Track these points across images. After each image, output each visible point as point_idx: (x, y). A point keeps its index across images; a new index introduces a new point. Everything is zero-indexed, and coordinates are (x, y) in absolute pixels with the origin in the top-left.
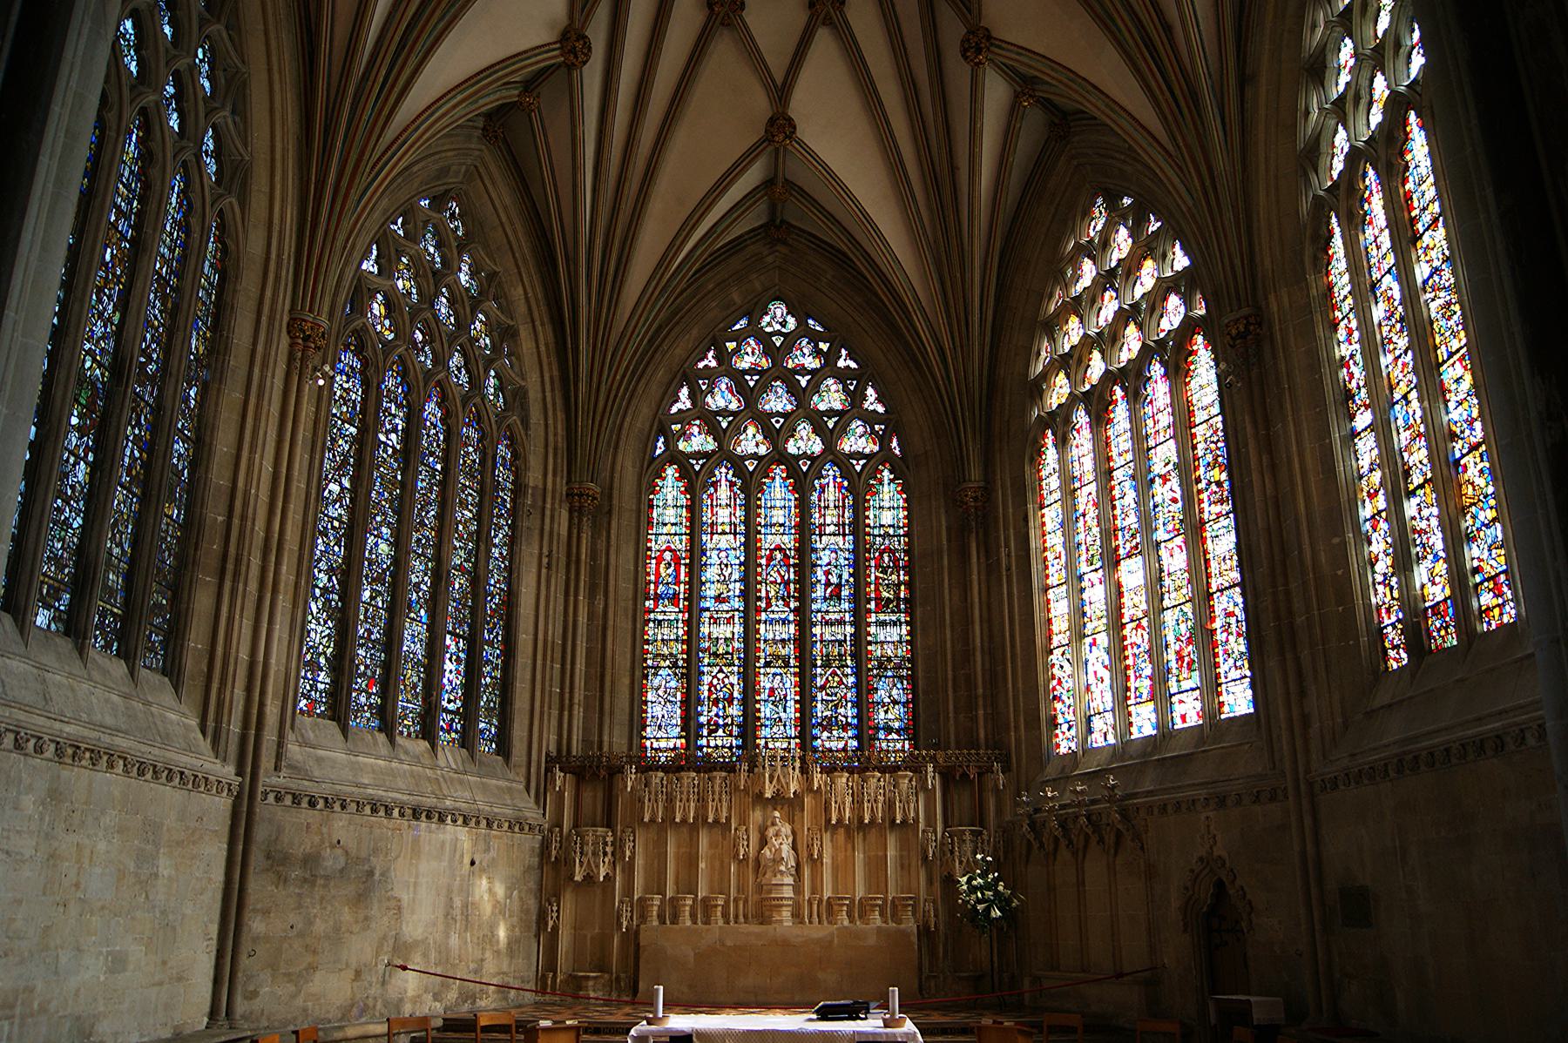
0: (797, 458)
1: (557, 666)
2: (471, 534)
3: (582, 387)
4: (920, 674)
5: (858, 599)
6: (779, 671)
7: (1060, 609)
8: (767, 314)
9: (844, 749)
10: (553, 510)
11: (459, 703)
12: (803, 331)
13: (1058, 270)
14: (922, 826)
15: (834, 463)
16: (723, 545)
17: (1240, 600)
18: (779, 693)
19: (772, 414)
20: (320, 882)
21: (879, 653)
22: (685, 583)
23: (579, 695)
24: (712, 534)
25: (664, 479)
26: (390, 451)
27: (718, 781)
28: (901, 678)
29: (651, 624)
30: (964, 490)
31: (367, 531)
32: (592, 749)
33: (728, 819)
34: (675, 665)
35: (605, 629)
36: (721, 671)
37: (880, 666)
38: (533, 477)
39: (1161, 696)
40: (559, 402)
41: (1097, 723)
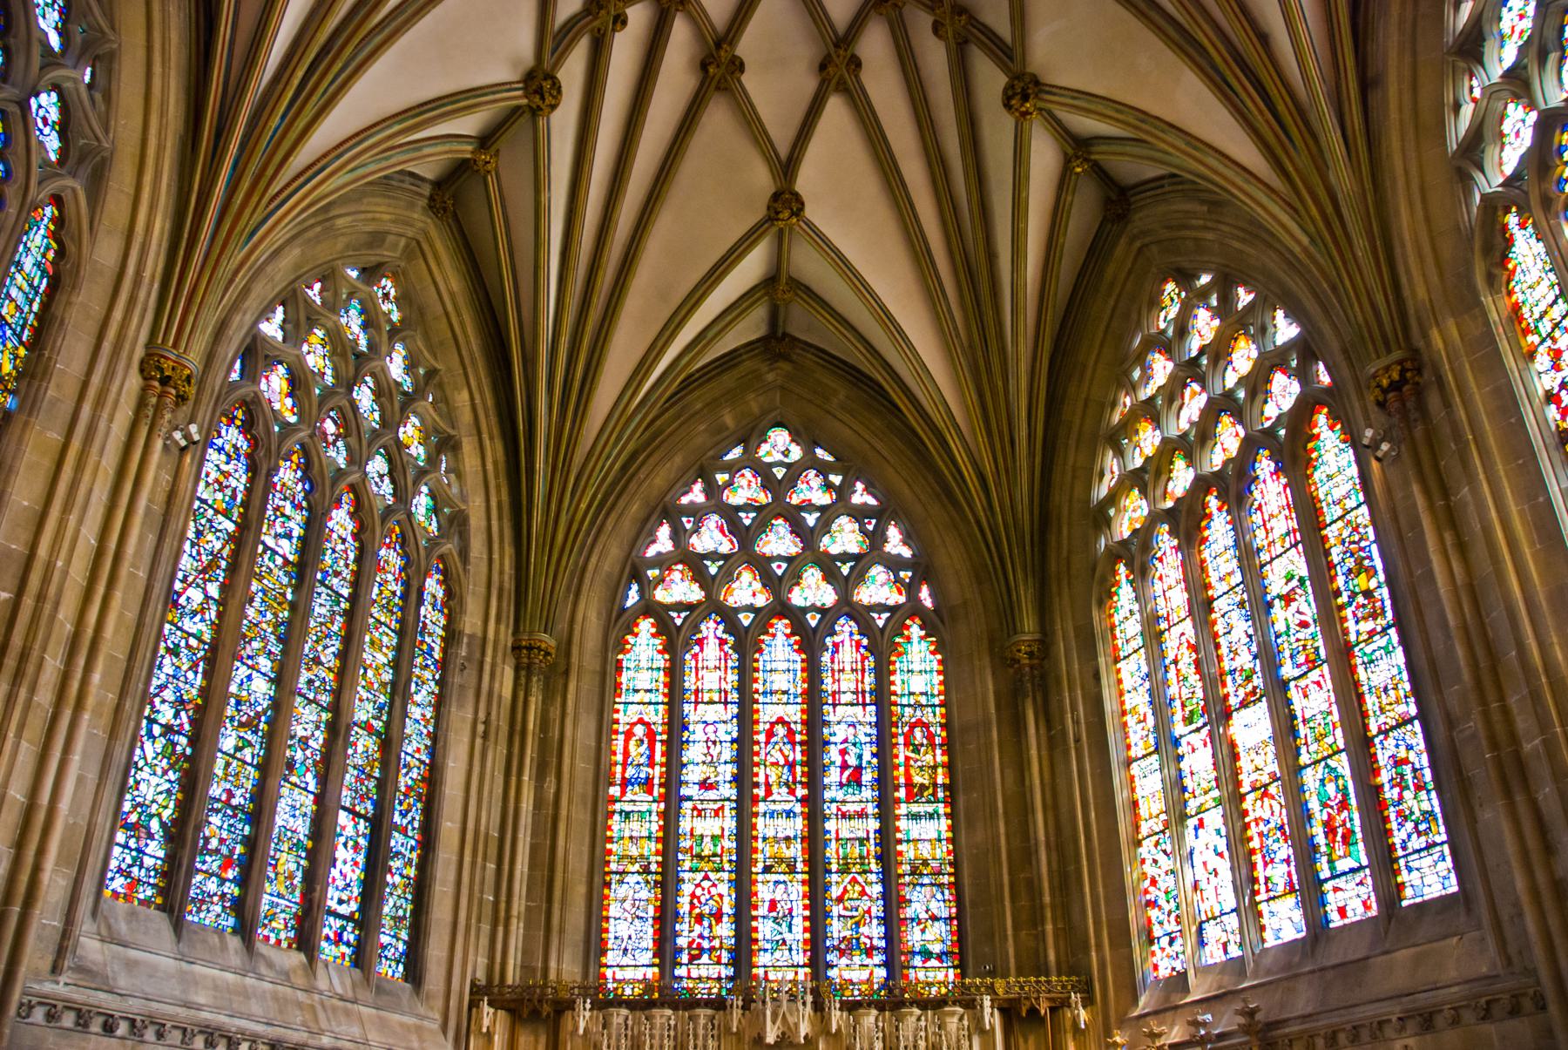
0: (804, 610)
1: (491, 866)
4: (966, 881)
5: (884, 783)
6: (782, 878)
8: (766, 441)
9: (869, 981)
10: (493, 665)
12: (809, 462)
15: (850, 616)
16: (710, 718)
19: (772, 559)
21: (911, 855)
22: (662, 765)
23: (519, 905)
24: (697, 703)
25: (636, 635)
27: (702, 1021)
29: (616, 817)
30: (1017, 643)
32: (534, 977)
34: (646, 870)
36: (706, 878)
38: (471, 623)
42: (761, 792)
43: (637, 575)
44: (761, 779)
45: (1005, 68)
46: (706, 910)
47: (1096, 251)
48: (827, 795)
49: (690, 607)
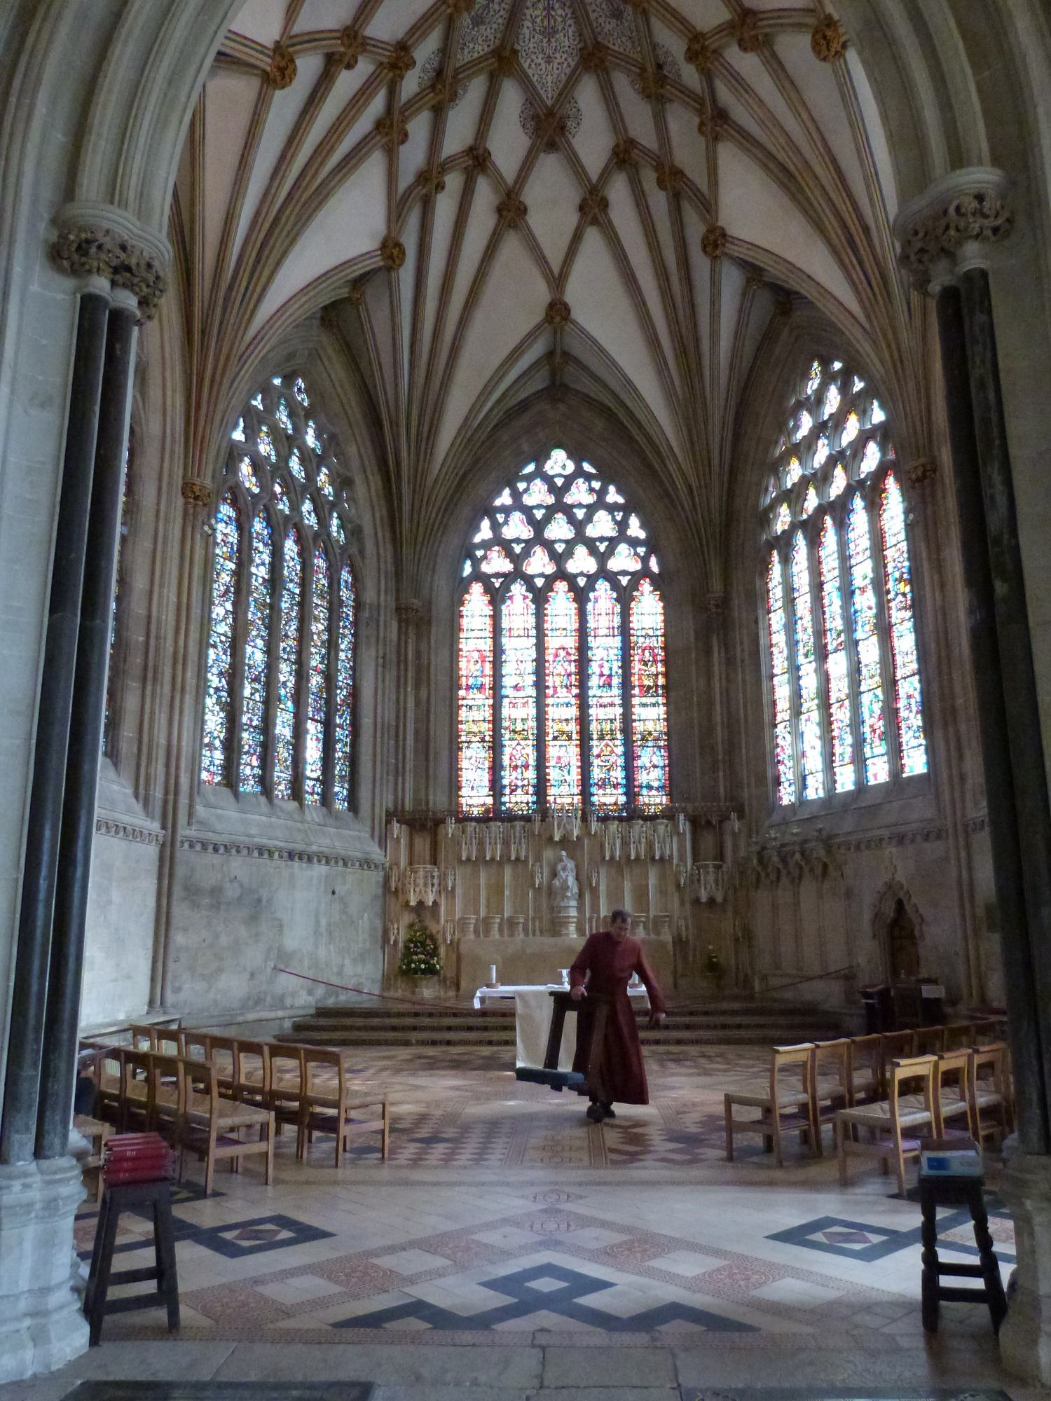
1: (392, 742)
2: (323, 642)
3: (406, 524)
5: (626, 686)
7: (782, 692)
9: (616, 804)
11: (319, 773)
12: (579, 473)
13: (782, 420)
14: (675, 861)
17: (918, 686)
18: (564, 761)
20: (223, 907)
23: (409, 765)
26: (260, 580)
28: (659, 747)
31: (246, 642)
33: (527, 857)
34: (483, 740)
35: (428, 711)
37: (644, 739)
38: (369, 596)
39: (859, 761)
40: (388, 535)
41: (810, 781)
42: (550, 692)
43: (471, 556)
44: (550, 683)
45: (704, 220)
46: (519, 763)
47: (768, 338)
48: (591, 693)
49: (504, 575)
